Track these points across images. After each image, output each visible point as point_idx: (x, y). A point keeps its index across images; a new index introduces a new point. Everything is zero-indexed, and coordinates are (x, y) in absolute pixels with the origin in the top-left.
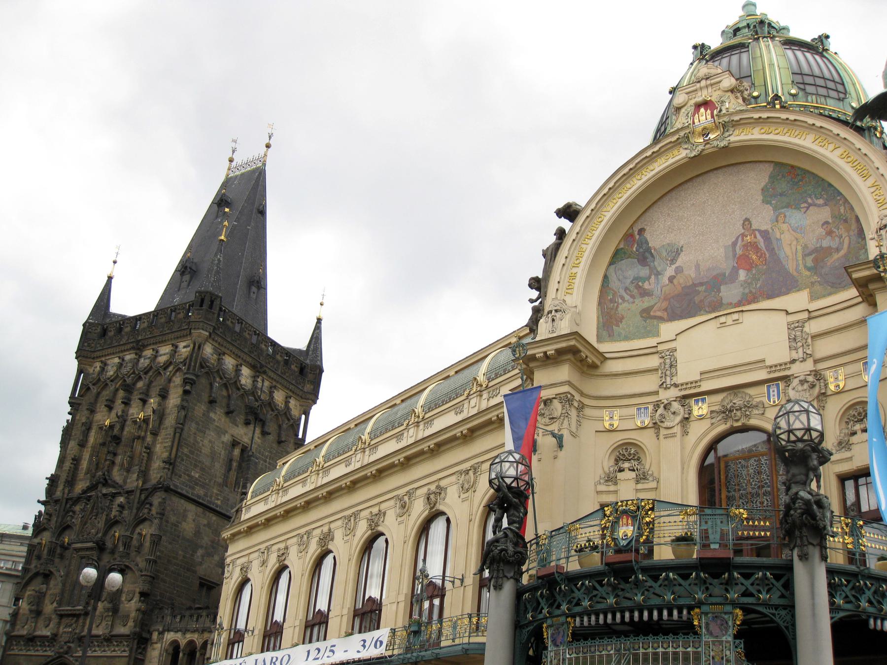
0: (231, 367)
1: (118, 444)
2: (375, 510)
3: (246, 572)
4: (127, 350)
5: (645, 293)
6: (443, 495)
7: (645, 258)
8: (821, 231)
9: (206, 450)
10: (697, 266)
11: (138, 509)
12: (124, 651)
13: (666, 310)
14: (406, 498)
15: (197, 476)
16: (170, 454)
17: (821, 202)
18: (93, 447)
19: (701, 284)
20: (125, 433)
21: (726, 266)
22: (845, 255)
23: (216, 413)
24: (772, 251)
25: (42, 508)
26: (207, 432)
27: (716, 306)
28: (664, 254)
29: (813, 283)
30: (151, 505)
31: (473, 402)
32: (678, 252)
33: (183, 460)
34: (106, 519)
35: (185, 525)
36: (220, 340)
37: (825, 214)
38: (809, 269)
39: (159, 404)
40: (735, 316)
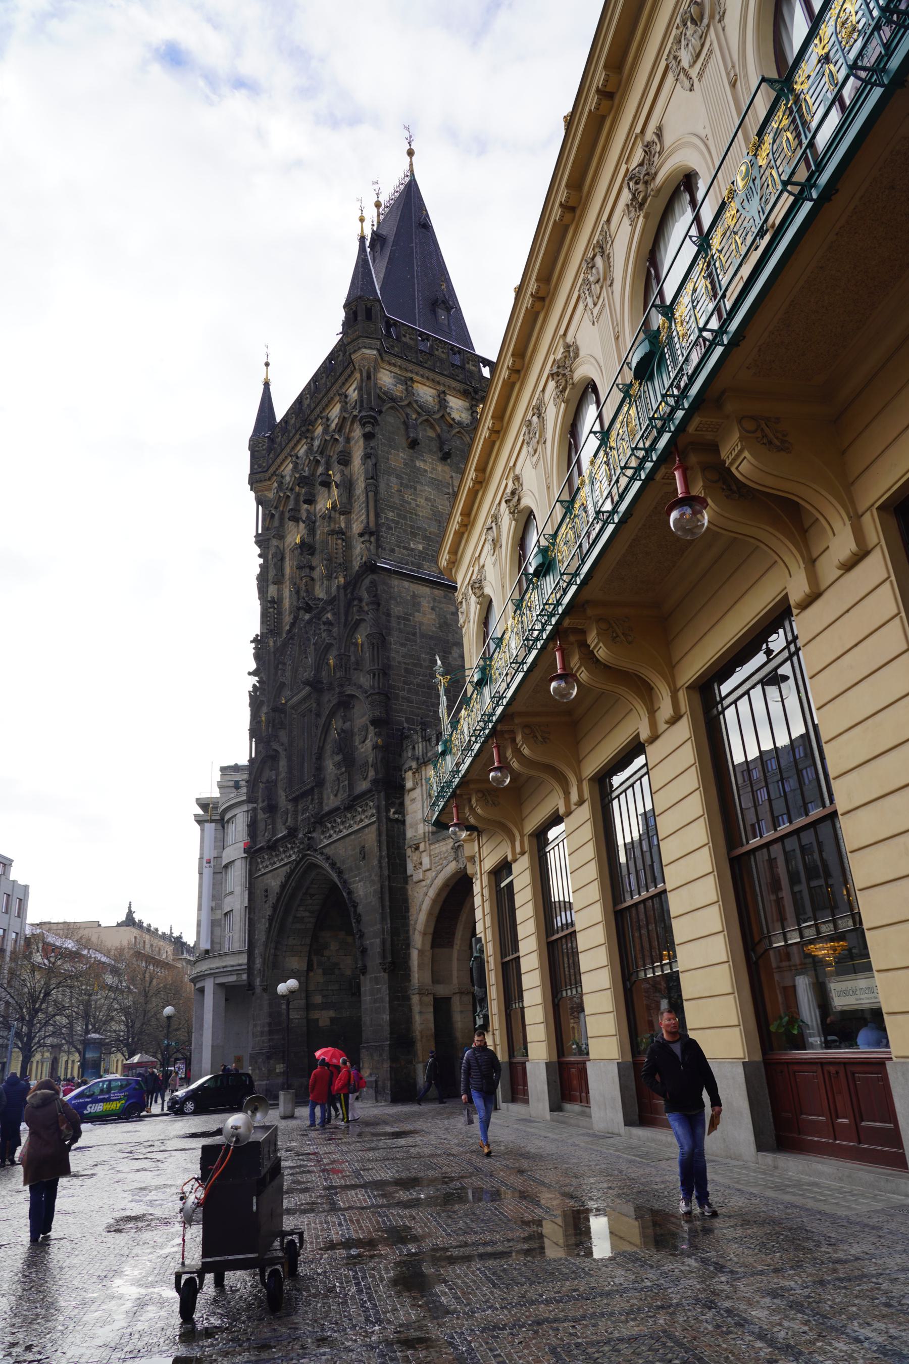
0: (430, 399)
1: (312, 554)
3: (481, 588)
4: (298, 441)
9: (424, 511)
11: (347, 614)
12: (372, 815)
15: (420, 547)
16: (368, 523)
18: (292, 578)
20: (317, 537)
23: (425, 461)
25: (254, 680)
26: (419, 487)
30: (361, 600)
33: (390, 528)
34: (315, 649)
35: (418, 617)
36: (399, 362)
39: (342, 473)
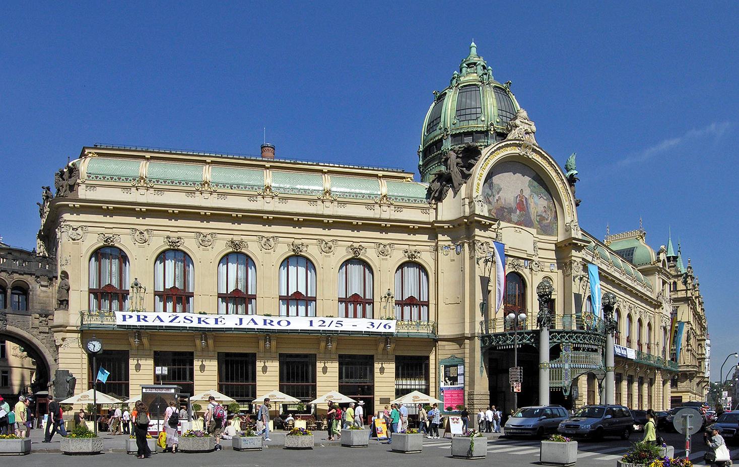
2: (299, 242)
5: (490, 203)
6: (363, 251)
7: (491, 186)
8: (542, 209)
10: (505, 200)
13: (495, 214)
14: (330, 244)
17: (545, 198)
19: (506, 209)
21: (514, 205)
22: (549, 223)
24: (527, 207)
27: (510, 221)
28: (496, 188)
29: (538, 228)
31: (385, 208)
32: (500, 190)
37: (545, 203)
38: (537, 222)
40: (520, 230)
